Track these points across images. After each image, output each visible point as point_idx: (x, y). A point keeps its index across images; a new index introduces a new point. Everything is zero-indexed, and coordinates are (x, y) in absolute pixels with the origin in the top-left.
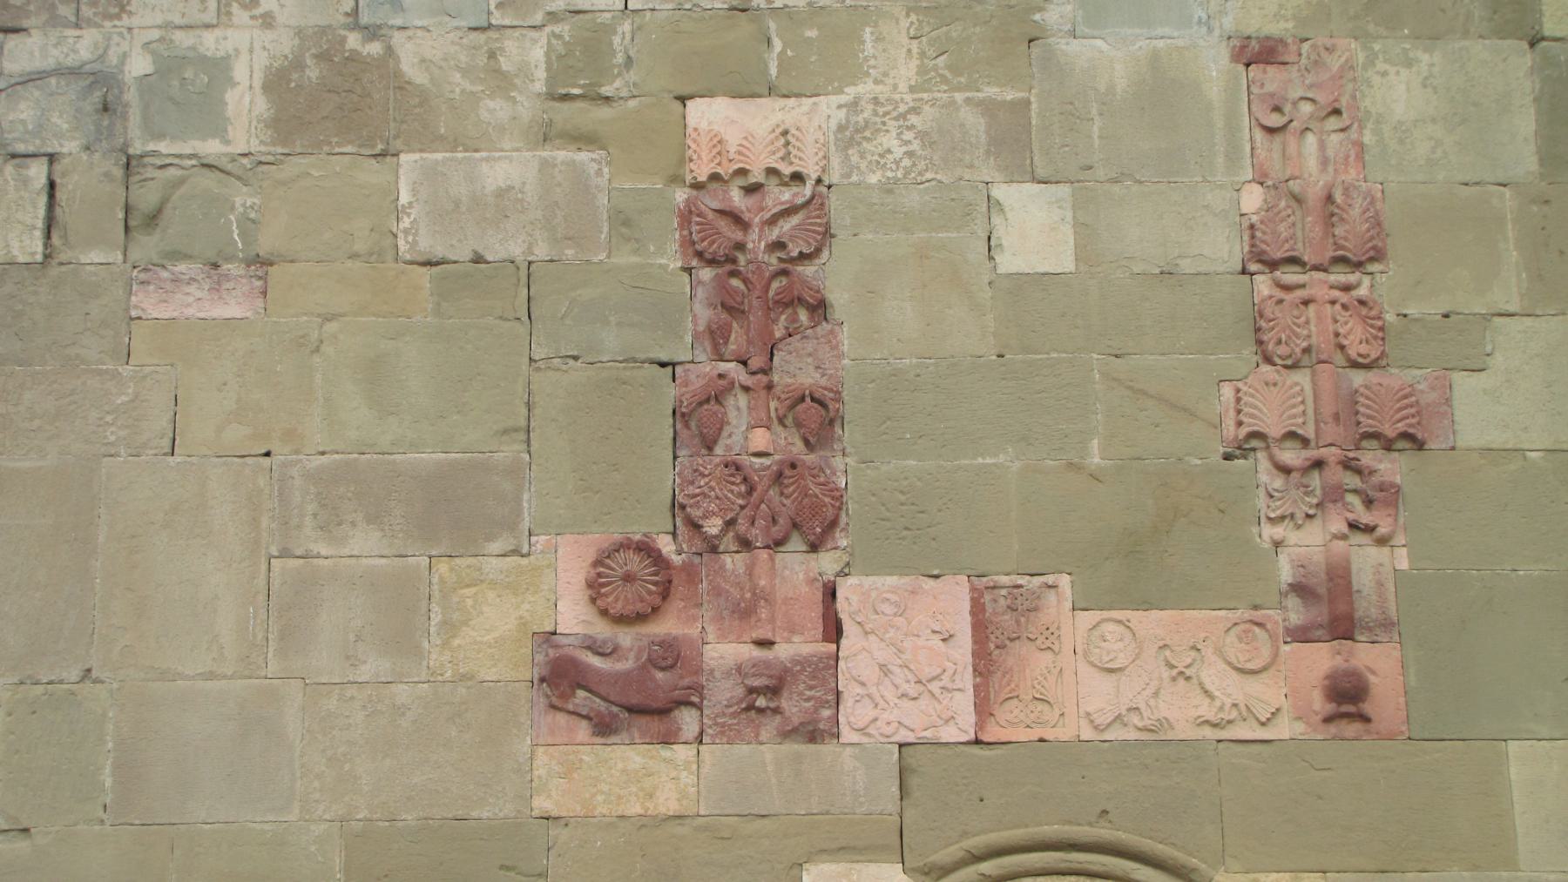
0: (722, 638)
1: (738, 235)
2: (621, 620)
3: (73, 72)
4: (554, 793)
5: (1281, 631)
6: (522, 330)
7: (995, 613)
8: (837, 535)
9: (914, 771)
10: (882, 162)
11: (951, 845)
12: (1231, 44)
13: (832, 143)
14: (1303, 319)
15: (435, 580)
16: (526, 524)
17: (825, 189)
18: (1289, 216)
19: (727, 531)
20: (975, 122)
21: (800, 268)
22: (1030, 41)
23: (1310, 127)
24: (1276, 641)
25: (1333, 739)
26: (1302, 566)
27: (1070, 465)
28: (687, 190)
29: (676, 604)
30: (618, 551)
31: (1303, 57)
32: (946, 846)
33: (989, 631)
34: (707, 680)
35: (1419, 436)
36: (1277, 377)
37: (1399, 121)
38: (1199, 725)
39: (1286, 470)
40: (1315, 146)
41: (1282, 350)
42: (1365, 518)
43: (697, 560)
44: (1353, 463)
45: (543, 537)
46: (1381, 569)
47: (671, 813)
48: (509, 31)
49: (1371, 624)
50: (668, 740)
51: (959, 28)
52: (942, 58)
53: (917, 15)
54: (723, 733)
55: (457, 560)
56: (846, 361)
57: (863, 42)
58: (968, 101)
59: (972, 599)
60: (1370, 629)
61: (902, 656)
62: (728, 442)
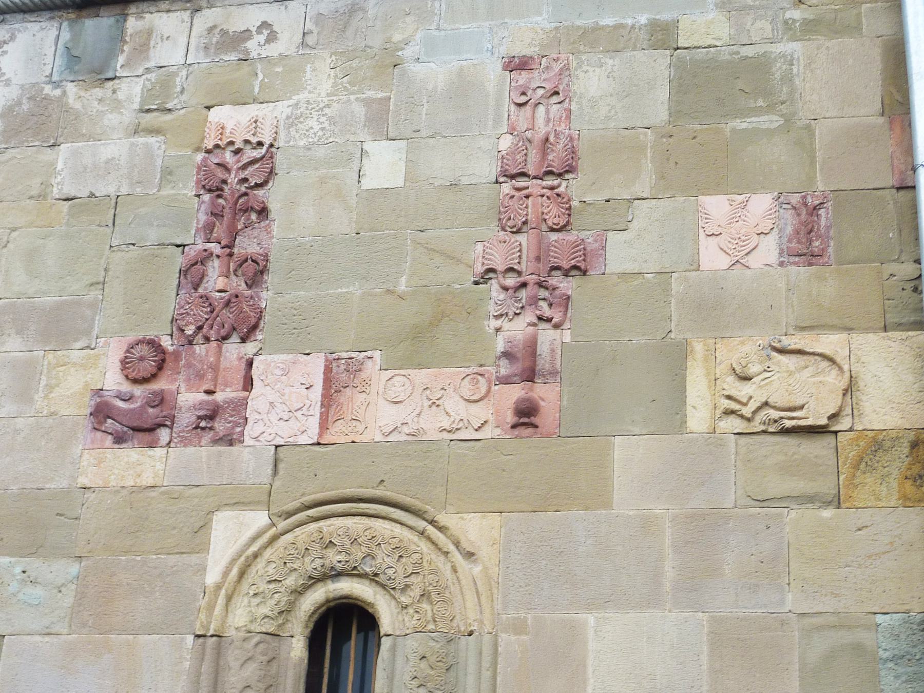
0: (189, 389)
2: (136, 381)
4: (89, 475)
5: (494, 378)
7: (337, 373)
8: (257, 333)
9: (282, 460)
10: (307, 133)
12: (503, 61)
14: (524, 206)
15: (46, 363)
18: (523, 150)
19: (198, 333)
20: (360, 111)
21: (255, 192)
22: (395, 66)
23: (541, 102)
26: (510, 342)
27: (388, 291)
29: (167, 372)
30: (137, 344)
33: (333, 382)
34: (178, 413)
35: (583, 267)
36: (507, 238)
38: (440, 431)
39: (506, 289)
40: (544, 112)
41: (510, 223)
42: (547, 312)
44: (544, 284)
45: (103, 339)
46: (554, 342)
47: (148, 485)
48: (125, 79)
49: (545, 373)
51: (357, 62)
53: (336, 56)
54: (181, 441)
55: (59, 353)
56: (274, 240)
57: (305, 72)
59: (325, 365)
60: (544, 376)
61: (283, 397)
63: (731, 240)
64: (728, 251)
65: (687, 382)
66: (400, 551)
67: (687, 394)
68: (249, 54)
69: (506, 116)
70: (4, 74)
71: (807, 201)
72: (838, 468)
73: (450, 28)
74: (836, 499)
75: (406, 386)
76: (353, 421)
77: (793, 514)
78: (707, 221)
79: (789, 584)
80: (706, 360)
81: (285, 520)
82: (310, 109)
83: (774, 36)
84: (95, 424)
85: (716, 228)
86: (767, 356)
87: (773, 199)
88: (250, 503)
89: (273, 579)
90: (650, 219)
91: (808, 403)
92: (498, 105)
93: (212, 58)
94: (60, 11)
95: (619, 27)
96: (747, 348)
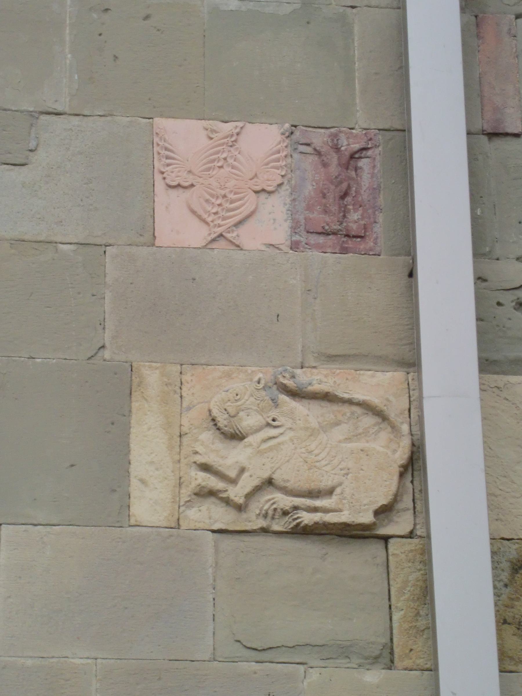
63: (211, 199)
64: (205, 216)
65: (132, 436)
67: (131, 457)
71: (340, 142)
72: (389, 599)
74: (386, 653)
77: (314, 675)
85: (185, 174)
86: (273, 400)
87: (283, 134)
90: (68, 149)
91: (340, 484)
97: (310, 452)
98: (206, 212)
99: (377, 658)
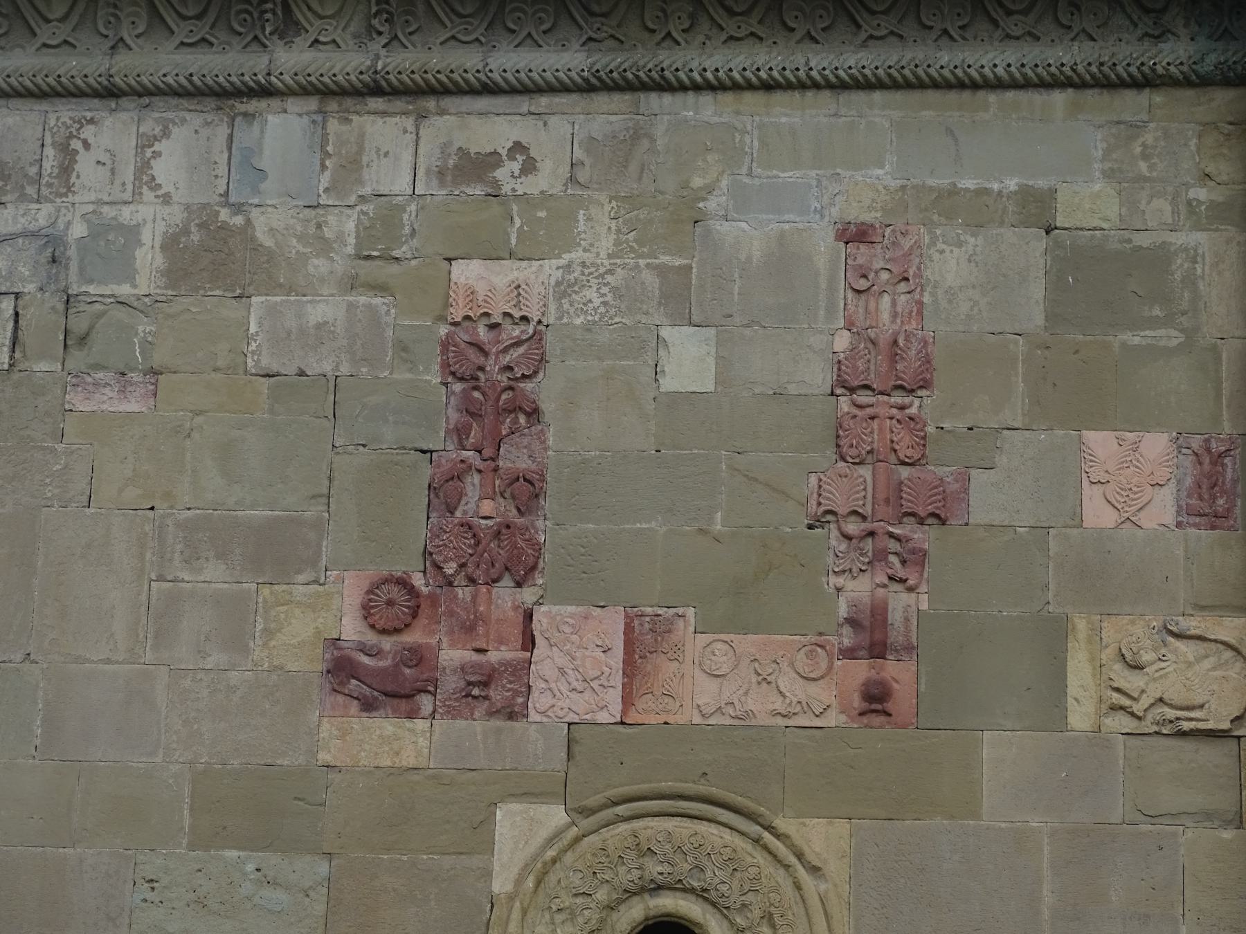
0: (452, 646)
1: (481, 360)
2: (384, 632)
3: (34, 235)
5: (836, 650)
6: (328, 424)
8: (536, 576)
9: (577, 742)
11: (599, 793)
13: (551, 294)
14: (869, 430)
15: (260, 600)
16: (324, 563)
17: (544, 328)
19: (460, 572)
21: (522, 385)
22: (696, 222)
24: (832, 658)
25: (865, 727)
28: (448, 326)
29: (422, 621)
31: (886, 238)
32: (595, 794)
35: (943, 516)
37: (950, 287)
39: (848, 538)
40: (889, 304)
41: (853, 452)
42: (900, 572)
43: (438, 591)
49: (899, 648)
50: (412, 715)
52: (632, 234)
53: (617, 202)
54: (449, 712)
56: (550, 453)
58: (648, 265)
60: (897, 651)
62: (465, 508)
64: (1117, 505)
65: (1068, 667)
66: (733, 864)
68: (501, 189)
69: (842, 305)
70: (160, 186)
72: (1240, 780)
73: (765, 175)
74: (1237, 818)
75: (729, 655)
76: (664, 696)
78: (1091, 464)
79: (1183, 915)
80: (1090, 641)
81: (588, 817)
82: (586, 274)
83: (1174, 220)
84: (335, 685)
85: (1102, 473)
88: (541, 794)
89: (581, 891)
91: (1208, 702)
92: (832, 289)
93: (450, 189)
94: (231, 99)
95: (982, 192)
96: (1139, 630)
97: (1187, 679)
98: (1117, 501)
99: (1230, 822)
